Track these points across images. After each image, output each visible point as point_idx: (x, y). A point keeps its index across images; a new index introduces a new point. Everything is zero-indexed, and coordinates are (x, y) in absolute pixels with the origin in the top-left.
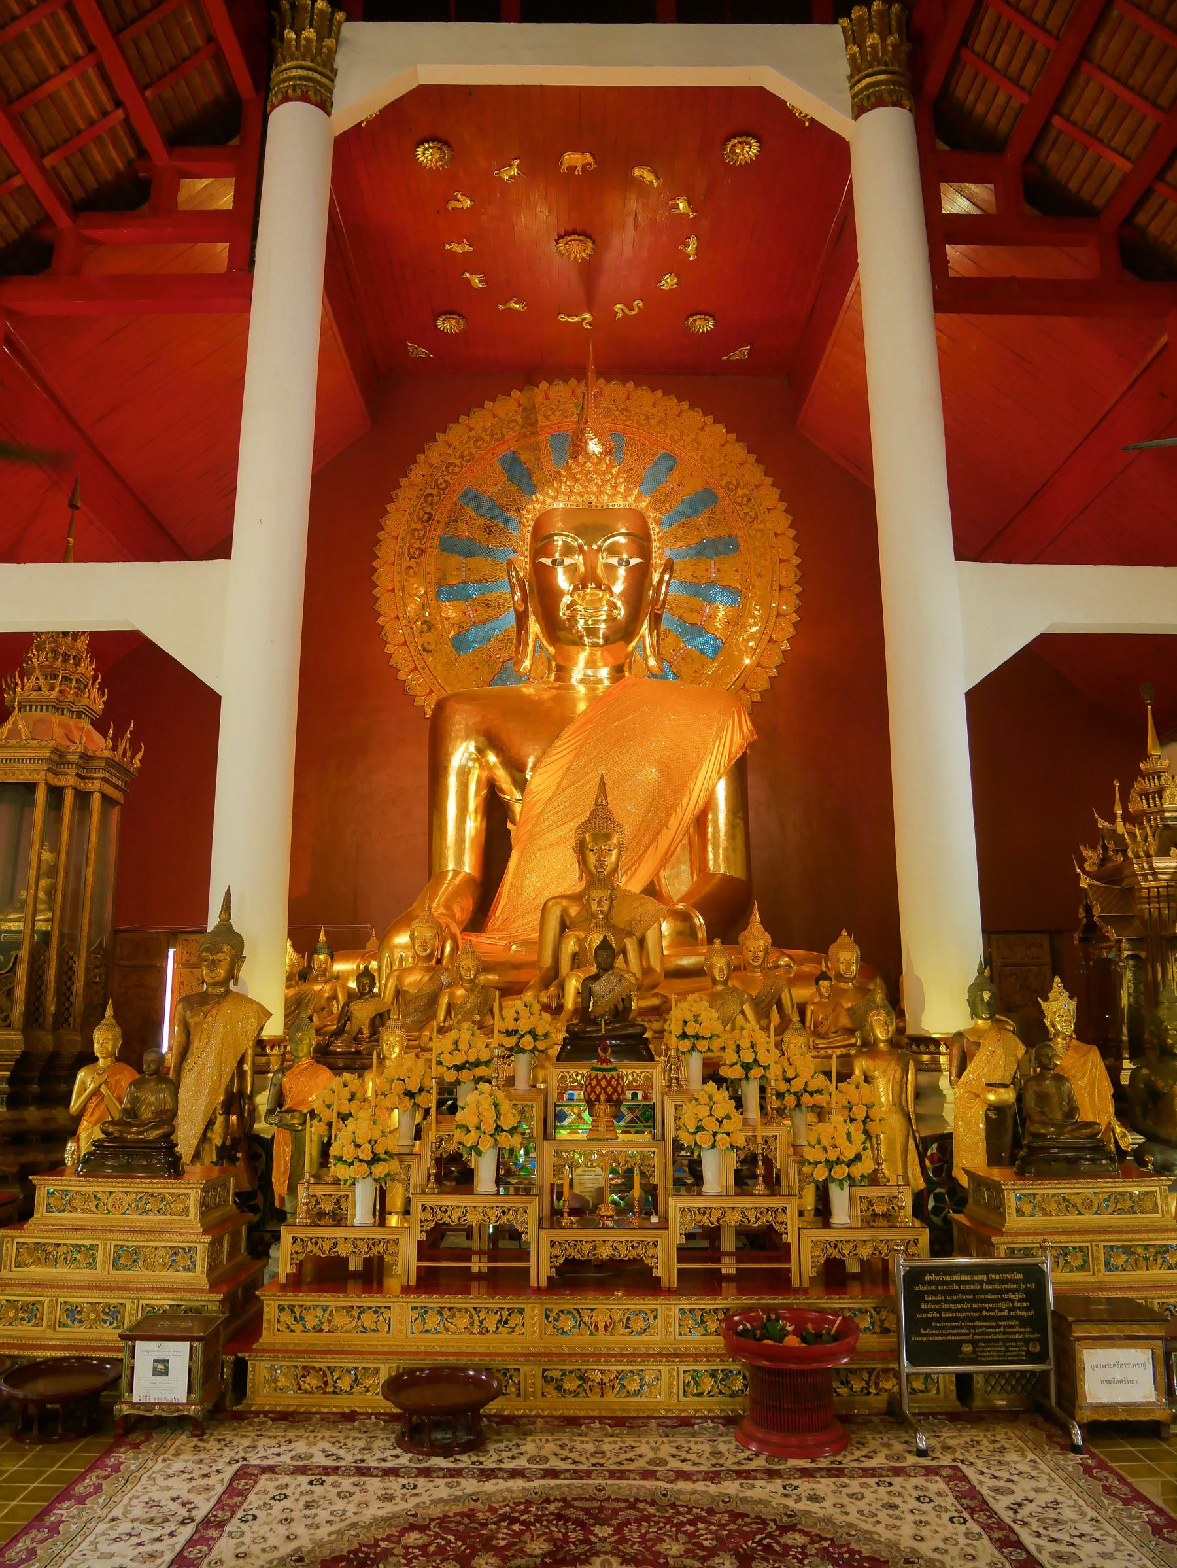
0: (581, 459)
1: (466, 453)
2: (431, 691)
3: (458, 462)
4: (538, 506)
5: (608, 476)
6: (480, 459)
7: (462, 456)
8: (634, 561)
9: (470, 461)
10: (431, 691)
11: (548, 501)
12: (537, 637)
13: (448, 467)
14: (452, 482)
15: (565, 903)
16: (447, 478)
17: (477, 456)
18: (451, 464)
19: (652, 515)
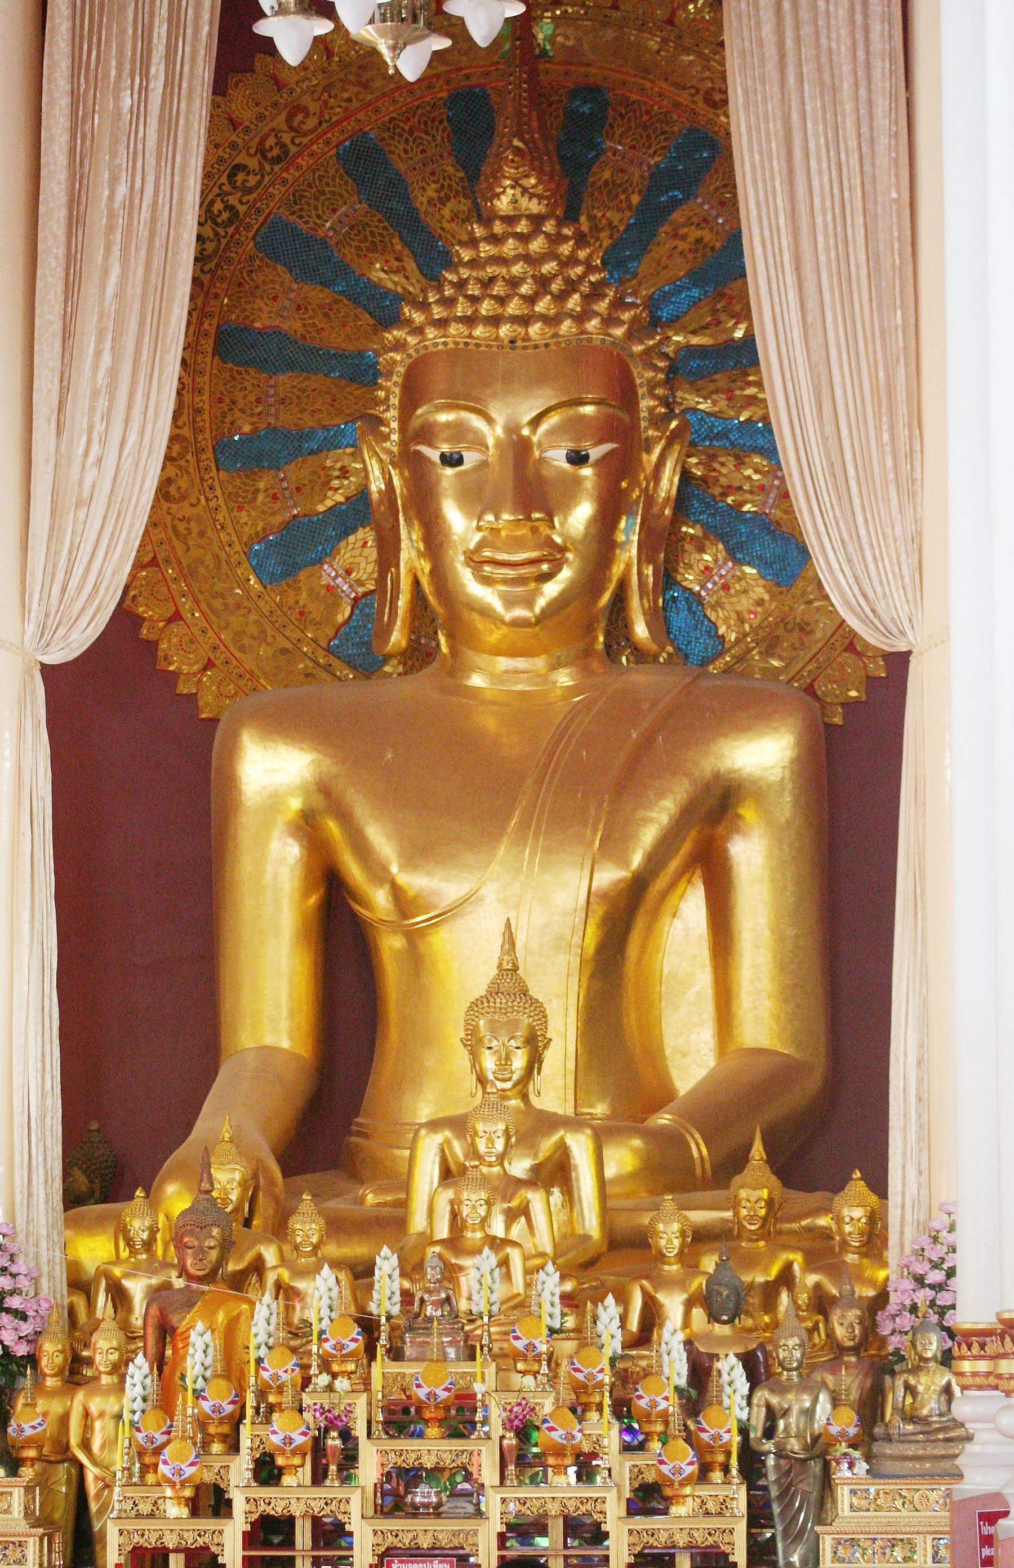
0: (498, 228)
1: (271, 141)
2: (209, 665)
3: (253, 163)
4: (412, 340)
5: (549, 267)
6: (300, 154)
7: (262, 151)
8: (596, 453)
9: (278, 160)
10: (209, 665)
11: (431, 333)
12: (416, 583)
13: (232, 176)
14: (242, 209)
15: (448, 1133)
16: (233, 200)
17: (293, 150)
18: (240, 168)
19: (638, 348)
